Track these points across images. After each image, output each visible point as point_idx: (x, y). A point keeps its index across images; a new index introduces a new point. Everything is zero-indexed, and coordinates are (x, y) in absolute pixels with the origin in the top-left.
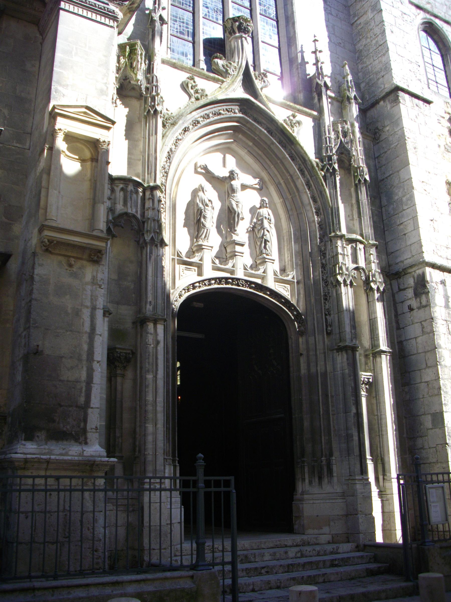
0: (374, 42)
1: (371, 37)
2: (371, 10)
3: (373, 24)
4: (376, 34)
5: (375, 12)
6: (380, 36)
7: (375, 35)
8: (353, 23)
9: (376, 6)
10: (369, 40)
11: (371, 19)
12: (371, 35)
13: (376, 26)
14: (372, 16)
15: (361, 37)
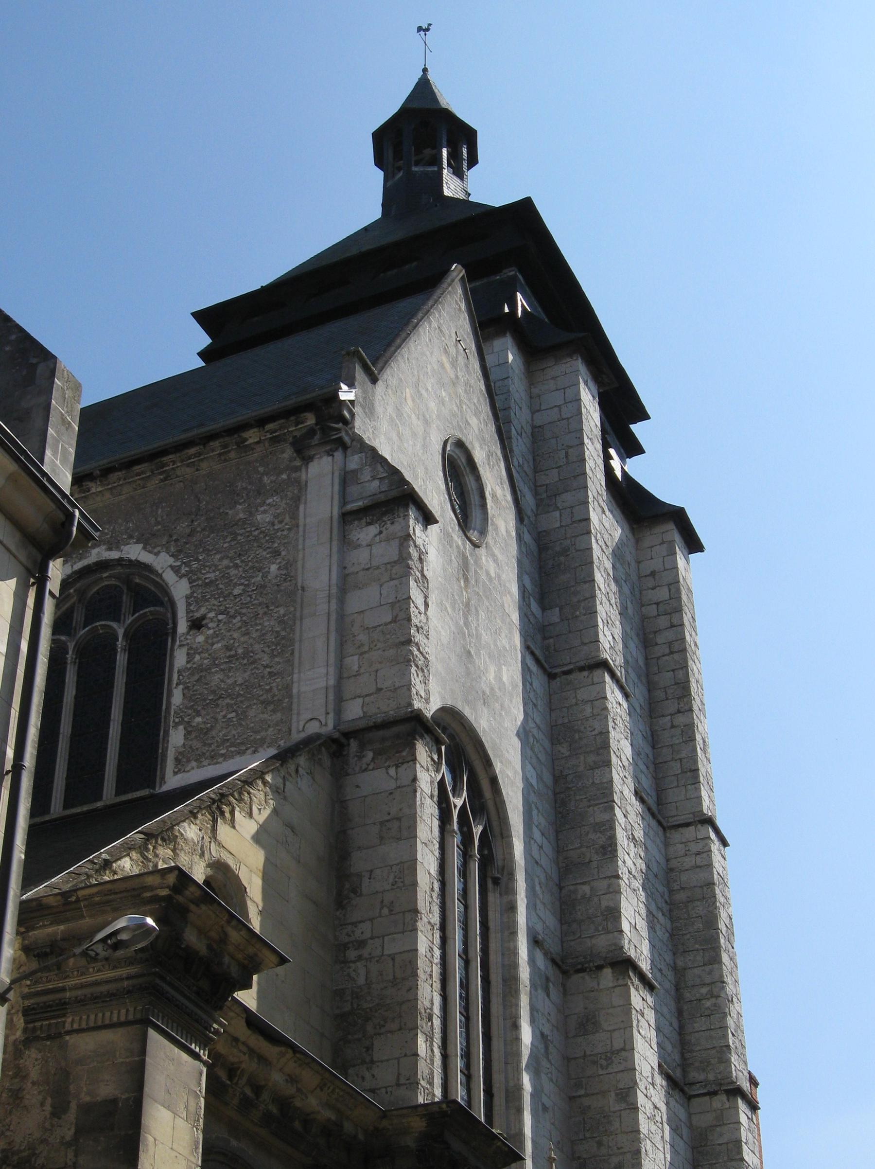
0: (615, 1160)
1: (609, 1147)
2: (617, 1095)
3: (616, 1124)
4: (622, 1148)
5: (624, 1105)
6: (629, 1156)
7: (618, 1149)
8: (574, 1097)
9: (627, 1095)
10: (603, 1150)
11: (614, 1112)
12: (610, 1144)
13: (622, 1132)
14: (617, 1108)
15: (588, 1135)
